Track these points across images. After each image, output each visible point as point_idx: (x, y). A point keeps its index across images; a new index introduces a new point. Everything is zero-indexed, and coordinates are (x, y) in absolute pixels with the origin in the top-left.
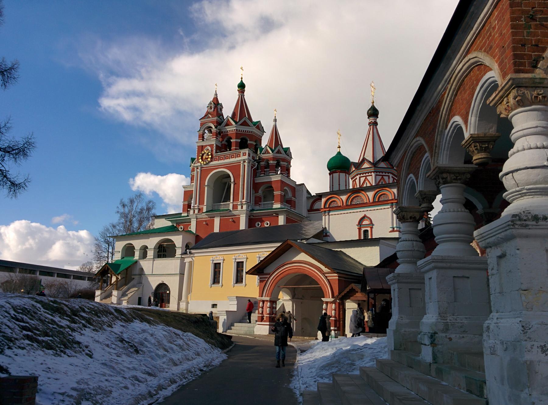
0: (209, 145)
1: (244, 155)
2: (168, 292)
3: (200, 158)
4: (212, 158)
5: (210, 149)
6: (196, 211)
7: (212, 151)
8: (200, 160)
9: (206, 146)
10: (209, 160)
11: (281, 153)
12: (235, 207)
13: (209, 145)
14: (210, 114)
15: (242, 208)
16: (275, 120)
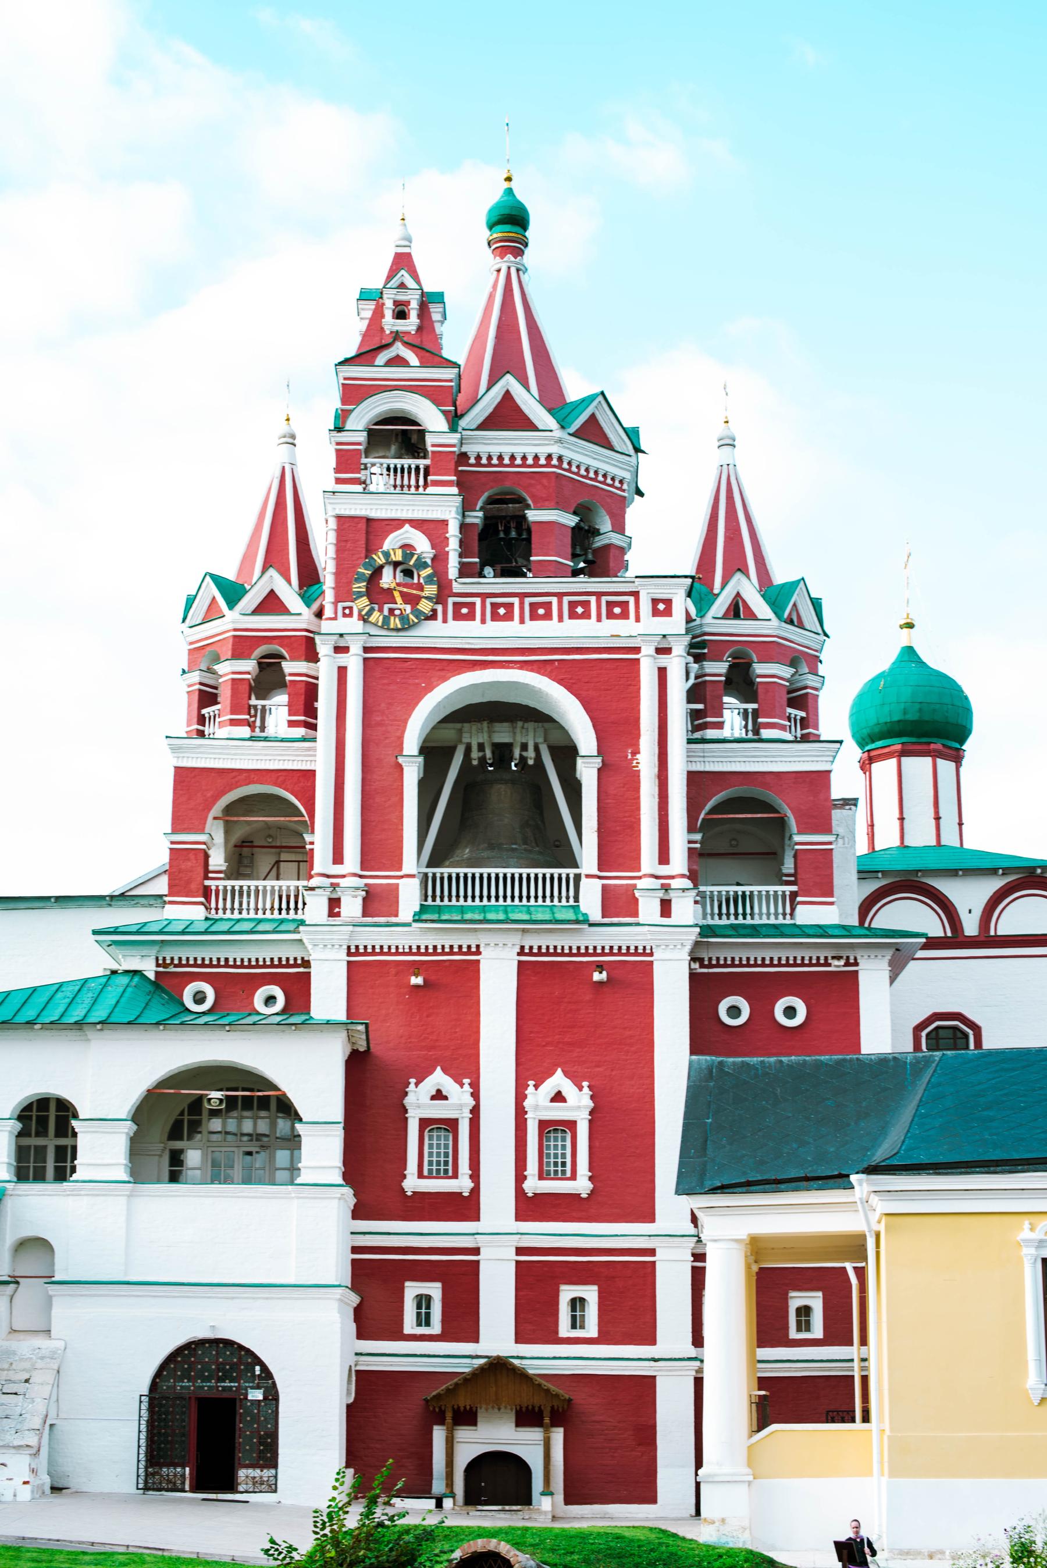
0: (418, 524)
1: (656, 613)
2: (256, 1395)
3: (360, 587)
4: (440, 598)
5: (423, 546)
6: (352, 907)
7: (440, 559)
8: (364, 601)
9: (397, 524)
10: (425, 606)
11: (801, 625)
12: (619, 904)
13: (418, 524)
14: (407, 344)
15: (666, 908)
16: (728, 443)
